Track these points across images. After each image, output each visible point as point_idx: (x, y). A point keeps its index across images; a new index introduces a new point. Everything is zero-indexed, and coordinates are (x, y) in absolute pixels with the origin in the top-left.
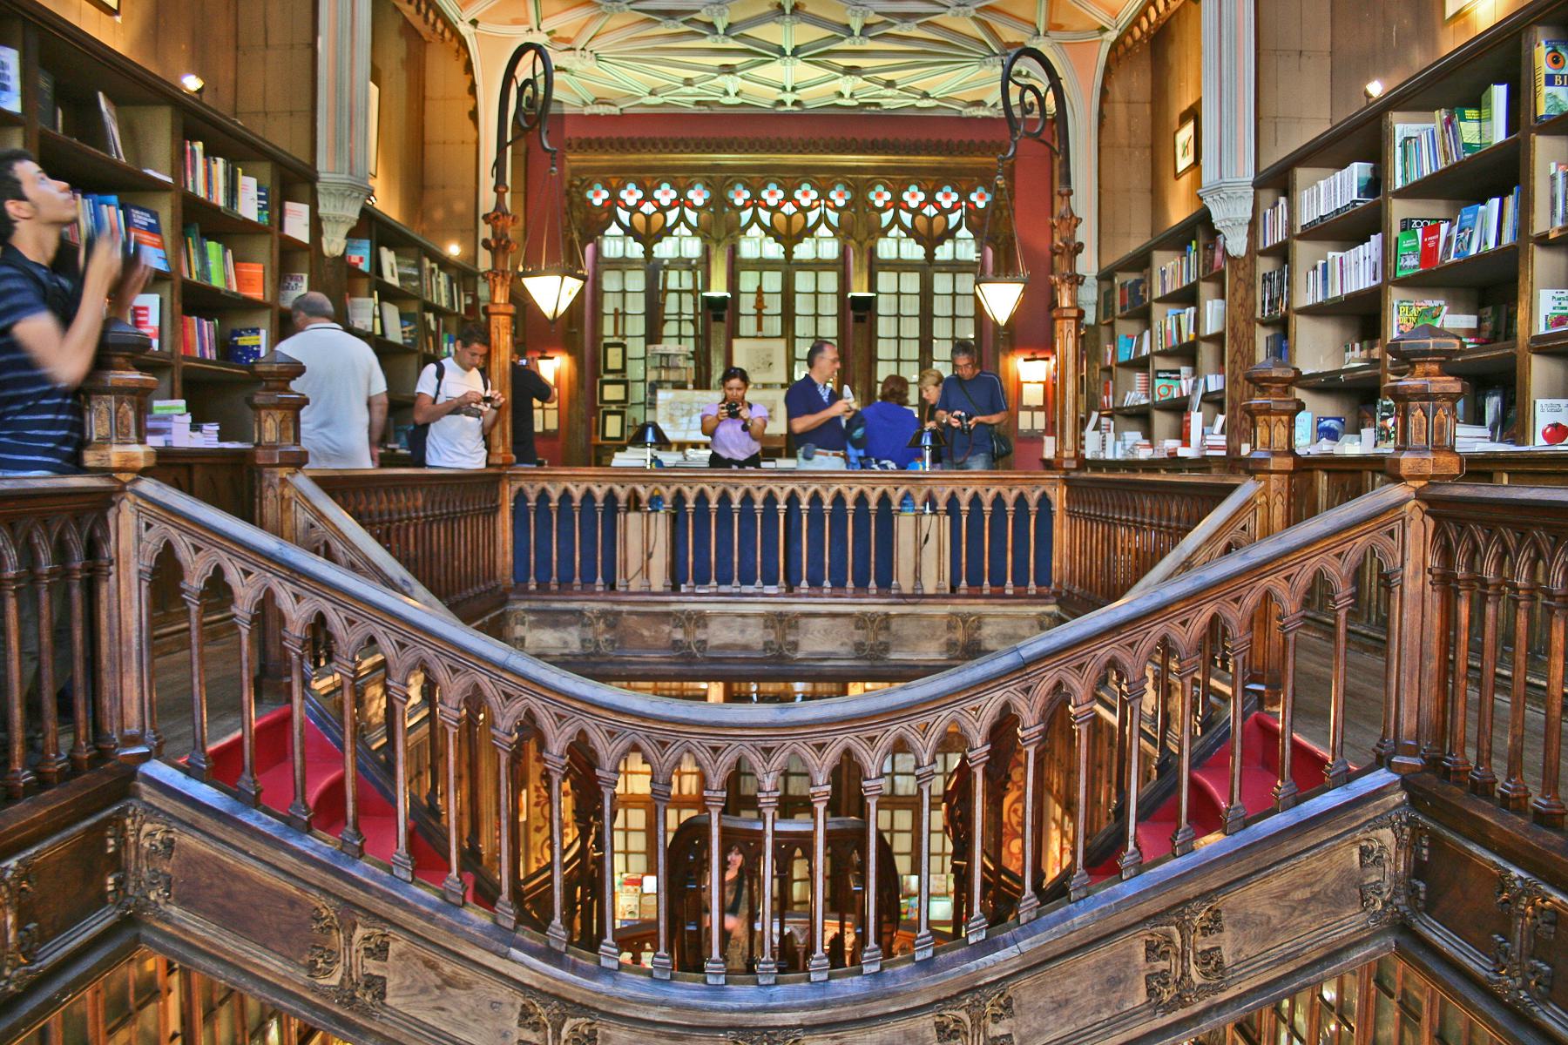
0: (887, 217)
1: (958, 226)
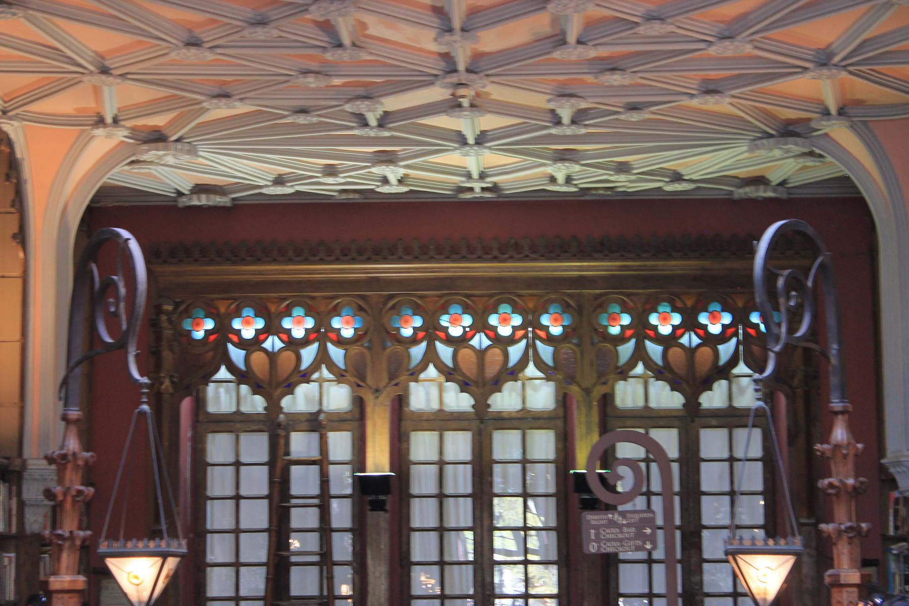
0: (626, 350)
1: (733, 361)
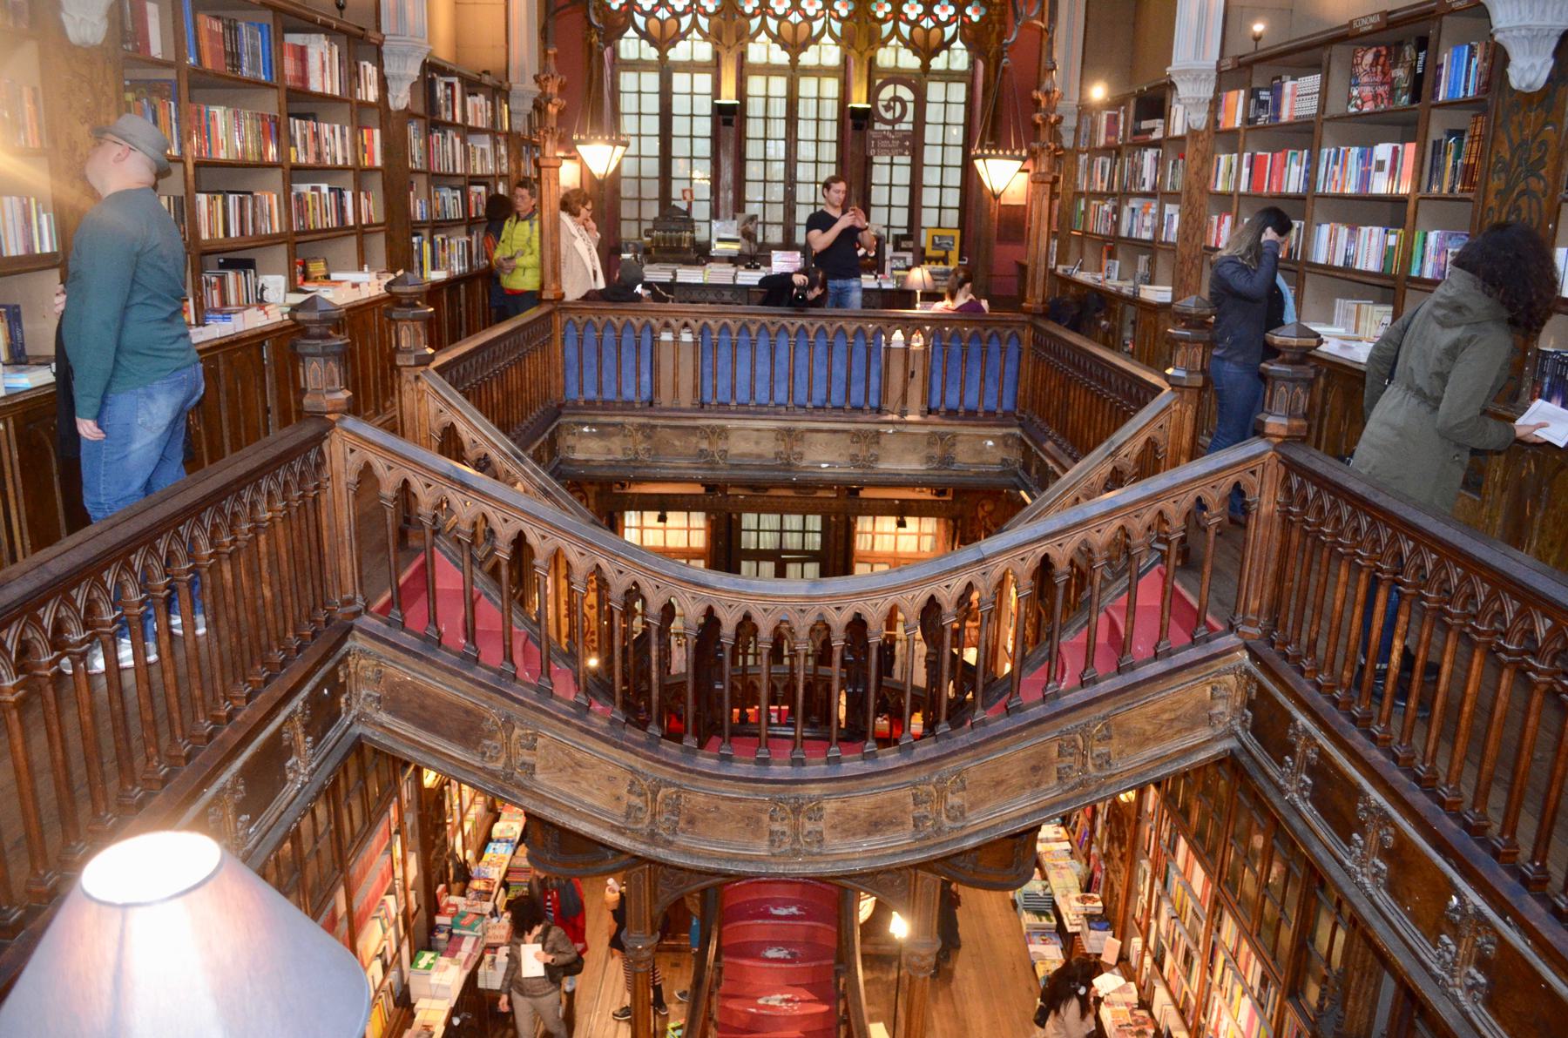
1: (953, 39)
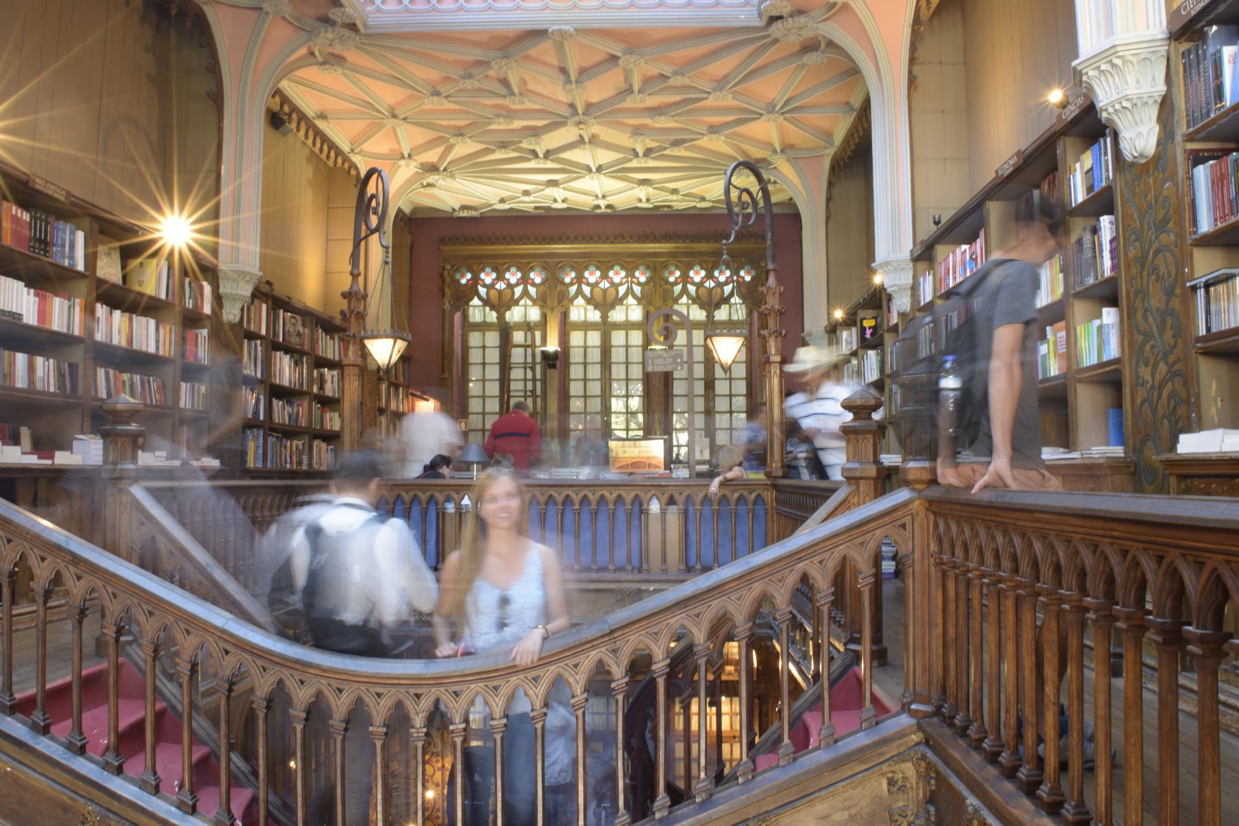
0: (678, 289)
1: (731, 295)
